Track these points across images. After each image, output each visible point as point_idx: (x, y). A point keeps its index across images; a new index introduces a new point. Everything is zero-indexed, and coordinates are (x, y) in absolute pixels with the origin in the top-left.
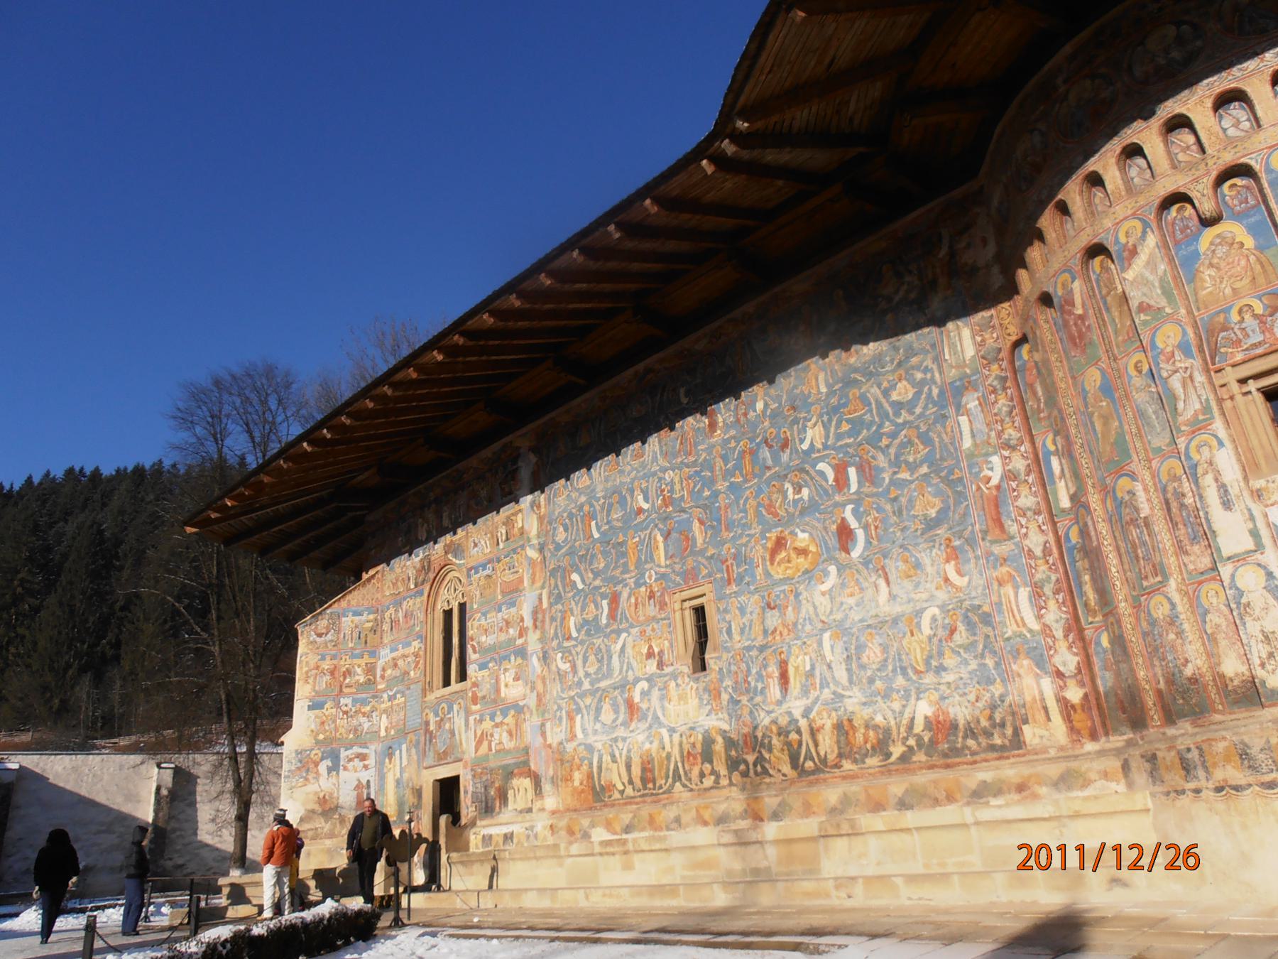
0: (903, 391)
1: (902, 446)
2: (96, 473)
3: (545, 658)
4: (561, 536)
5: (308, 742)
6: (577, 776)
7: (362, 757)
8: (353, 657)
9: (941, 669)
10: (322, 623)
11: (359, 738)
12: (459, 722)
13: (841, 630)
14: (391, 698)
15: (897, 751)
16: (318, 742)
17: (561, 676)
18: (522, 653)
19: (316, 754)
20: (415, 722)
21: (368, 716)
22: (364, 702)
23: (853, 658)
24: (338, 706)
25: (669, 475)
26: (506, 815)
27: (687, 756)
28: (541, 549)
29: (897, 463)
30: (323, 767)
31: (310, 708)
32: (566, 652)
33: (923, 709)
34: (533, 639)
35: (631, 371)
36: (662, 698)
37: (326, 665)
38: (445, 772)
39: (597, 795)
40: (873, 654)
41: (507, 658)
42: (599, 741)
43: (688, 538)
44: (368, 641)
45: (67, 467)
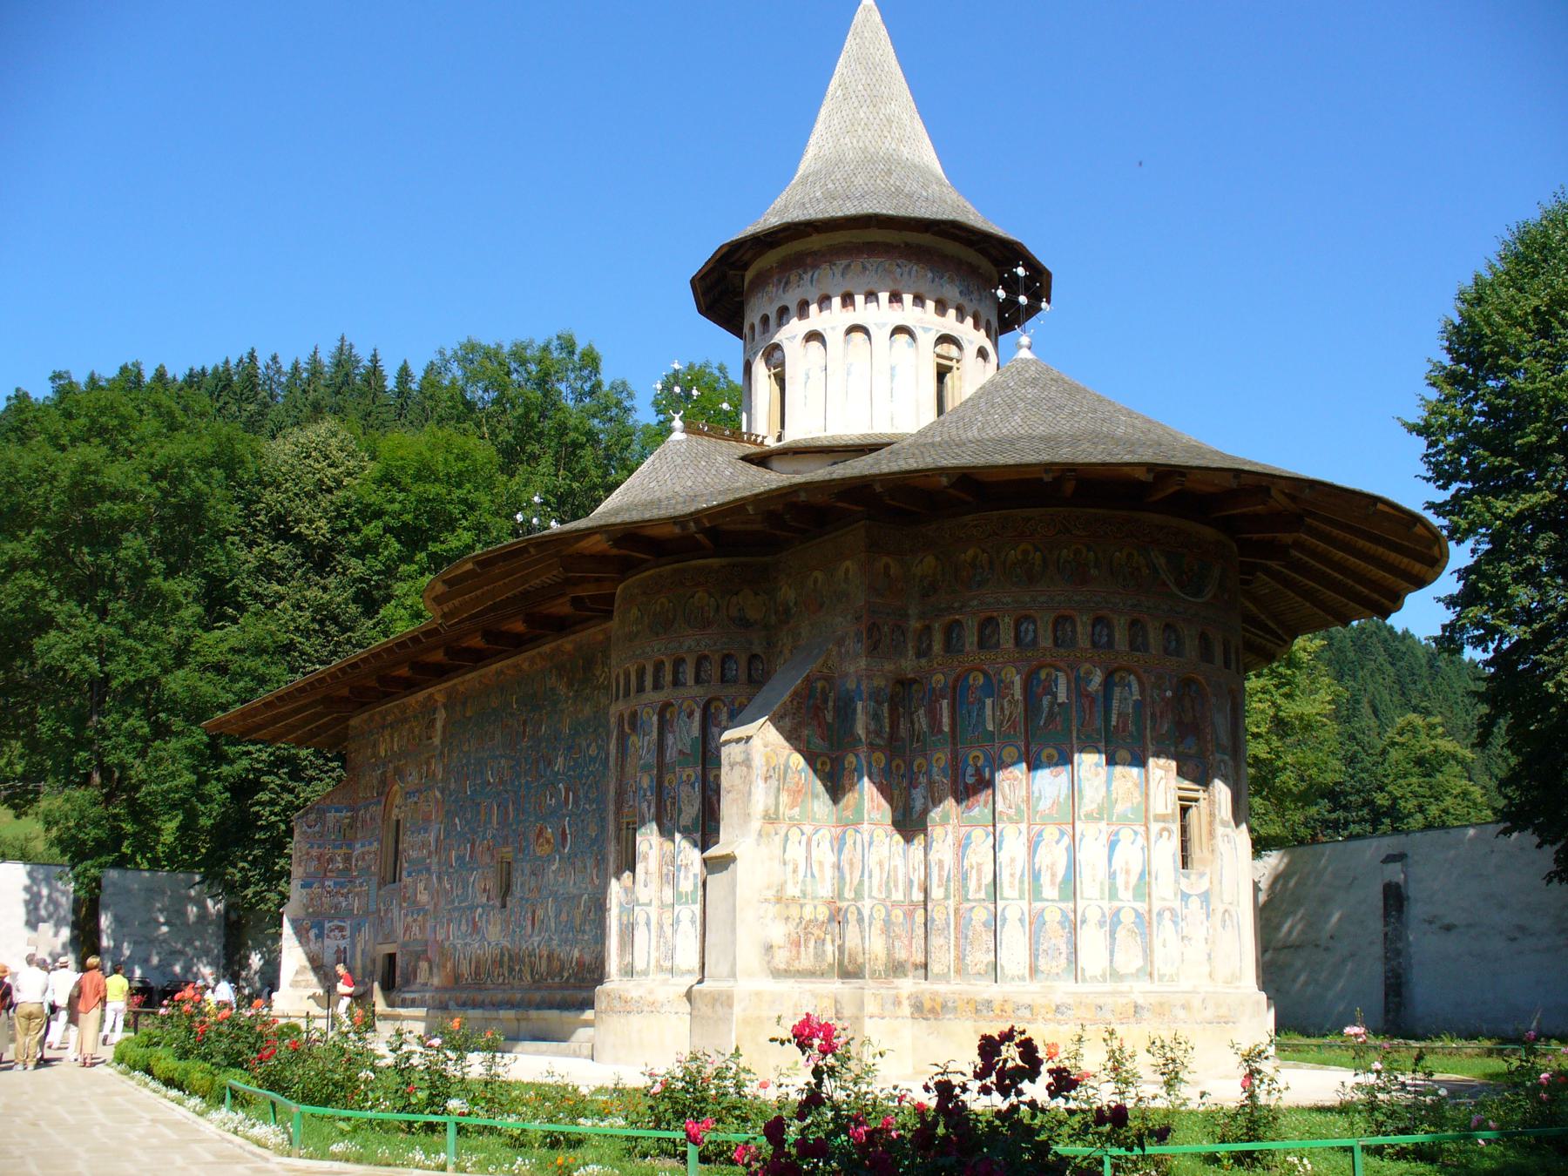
0: (593, 751)
1: (590, 786)
2: (160, 375)
3: (439, 878)
4: (453, 786)
5: (302, 914)
6: (449, 965)
7: (341, 929)
8: (335, 847)
9: (584, 932)
10: (312, 817)
11: (338, 913)
12: (396, 913)
13: (555, 900)
14: (361, 885)
15: (566, 975)
16: (308, 914)
17: (446, 892)
18: (428, 870)
19: (306, 924)
20: (373, 907)
21: (346, 896)
22: (342, 886)
23: (557, 916)
24: (323, 886)
25: (503, 762)
26: (414, 987)
27: (494, 962)
28: (442, 793)
29: (586, 797)
30: (312, 934)
31: (303, 886)
32: (449, 876)
33: (576, 954)
34: (435, 859)
35: (494, 667)
36: (488, 921)
37: (314, 852)
38: (389, 949)
39: (457, 978)
40: (564, 917)
41: (420, 872)
42: (459, 943)
43: (507, 813)
44: (347, 834)
45: (122, 364)
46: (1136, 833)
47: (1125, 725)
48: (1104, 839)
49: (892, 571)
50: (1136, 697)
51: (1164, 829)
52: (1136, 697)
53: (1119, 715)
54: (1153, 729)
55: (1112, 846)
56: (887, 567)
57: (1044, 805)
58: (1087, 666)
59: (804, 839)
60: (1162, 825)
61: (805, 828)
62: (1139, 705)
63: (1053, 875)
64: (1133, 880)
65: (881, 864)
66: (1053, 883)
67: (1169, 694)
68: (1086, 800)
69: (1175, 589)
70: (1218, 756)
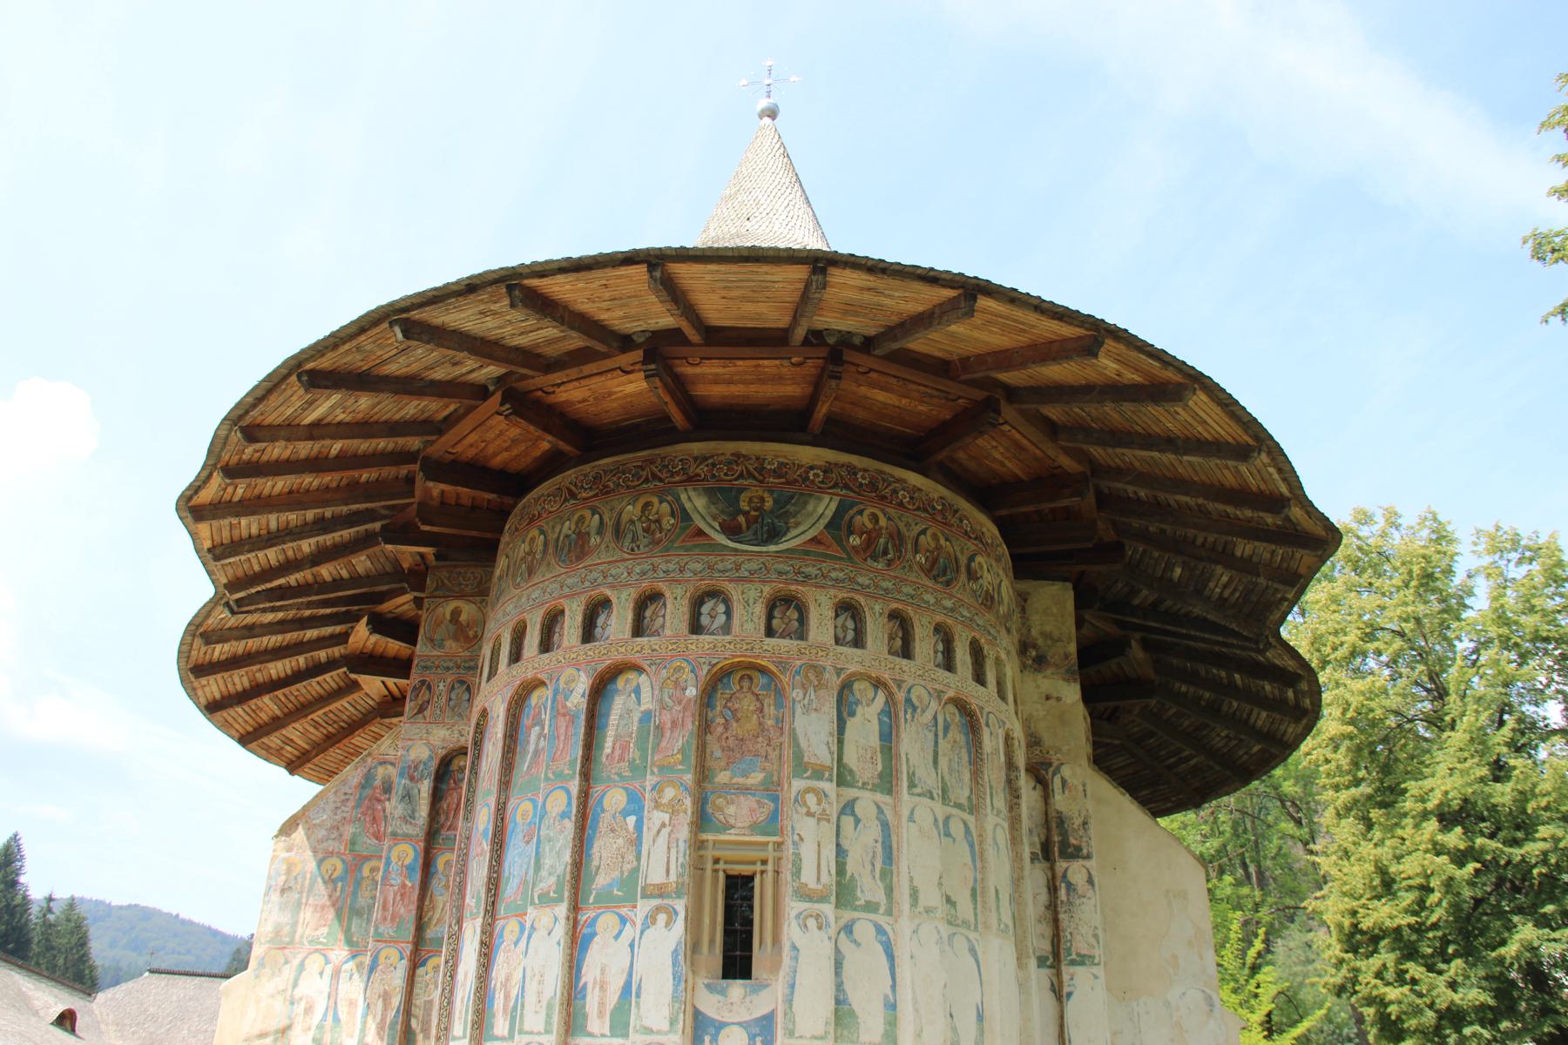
46: (623, 920)
47: (625, 748)
48: (560, 931)
49: (463, 618)
50: (647, 703)
51: (658, 909)
52: (647, 703)
53: (617, 737)
54: (657, 746)
55: (577, 942)
56: (456, 613)
57: (510, 889)
58: (571, 671)
59: (329, 970)
60: (656, 902)
61: (333, 955)
62: (647, 716)
63: (507, 997)
64: (613, 998)
65: (386, 997)
66: (505, 1010)
67: (692, 692)
68: (544, 873)
69: (721, 539)
70: (798, 784)
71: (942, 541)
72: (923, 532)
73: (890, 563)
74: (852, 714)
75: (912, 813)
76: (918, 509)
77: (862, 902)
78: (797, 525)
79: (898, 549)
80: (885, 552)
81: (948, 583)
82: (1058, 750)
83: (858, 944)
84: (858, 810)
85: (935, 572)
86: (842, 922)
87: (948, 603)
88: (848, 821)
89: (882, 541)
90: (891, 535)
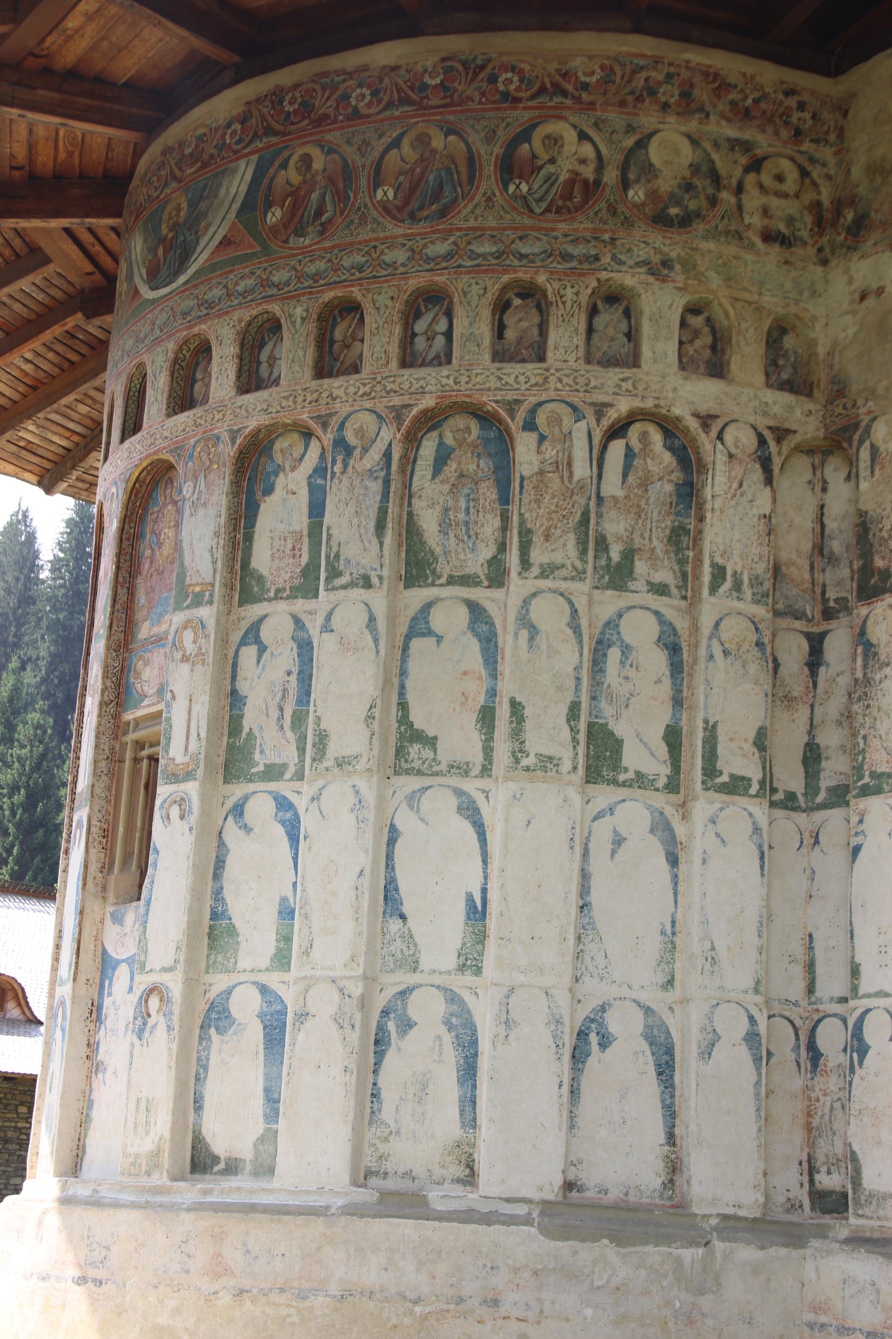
71: (438, 141)
72: (396, 143)
73: (324, 229)
74: (269, 490)
75: (328, 618)
76: (387, 107)
77: (261, 768)
78: (207, 228)
79: (342, 198)
80: (319, 213)
81: (443, 213)
82: (872, 393)
83: (247, 829)
84: (265, 634)
85: (414, 204)
86: (230, 803)
87: (441, 248)
88: (249, 653)
89: (315, 196)
90: (331, 180)
